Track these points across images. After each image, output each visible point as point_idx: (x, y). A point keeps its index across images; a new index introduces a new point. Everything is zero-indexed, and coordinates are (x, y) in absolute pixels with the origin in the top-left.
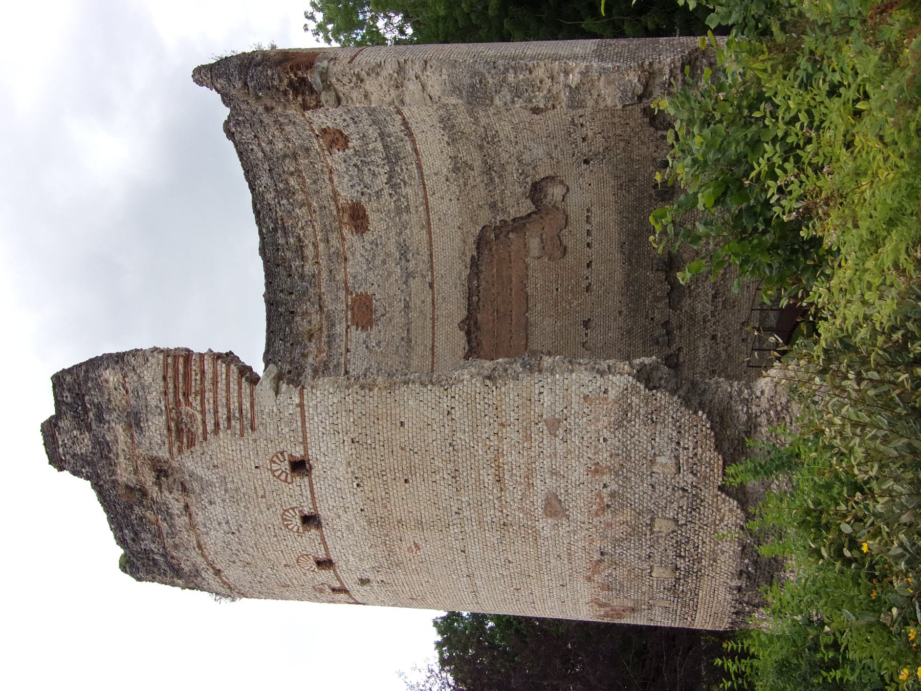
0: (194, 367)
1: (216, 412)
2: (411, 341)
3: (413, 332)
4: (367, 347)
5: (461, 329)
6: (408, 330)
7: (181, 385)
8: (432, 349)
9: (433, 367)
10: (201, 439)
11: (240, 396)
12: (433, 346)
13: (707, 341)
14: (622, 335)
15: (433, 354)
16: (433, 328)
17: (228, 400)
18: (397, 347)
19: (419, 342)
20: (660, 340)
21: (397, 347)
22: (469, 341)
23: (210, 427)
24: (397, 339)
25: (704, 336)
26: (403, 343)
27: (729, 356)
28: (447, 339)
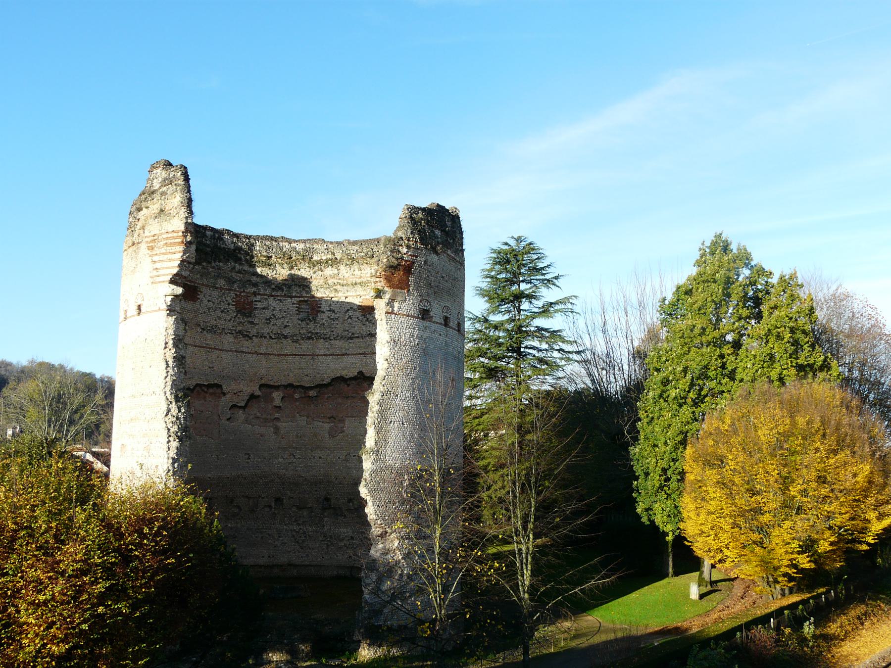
0: (177, 247)
1: (160, 261)
2: (351, 339)
3: (357, 340)
4: (348, 310)
5: (358, 373)
6: (358, 337)
7: (170, 241)
8: (346, 354)
9: (335, 355)
10: (150, 253)
11: (164, 275)
12: (349, 355)
13: (350, 534)
14: (354, 479)
15: (343, 355)
16: (360, 354)
17: (163, 268)
18: (348, 331)
19: (351, 345)
20: (351, 504)
21: (348, 331)
22: (351, 379)
23: (156, 258)
24: (353, 330)
25: (353, 532)
26: (350, 334)
27: (341, 548)
28: (353, 364)
